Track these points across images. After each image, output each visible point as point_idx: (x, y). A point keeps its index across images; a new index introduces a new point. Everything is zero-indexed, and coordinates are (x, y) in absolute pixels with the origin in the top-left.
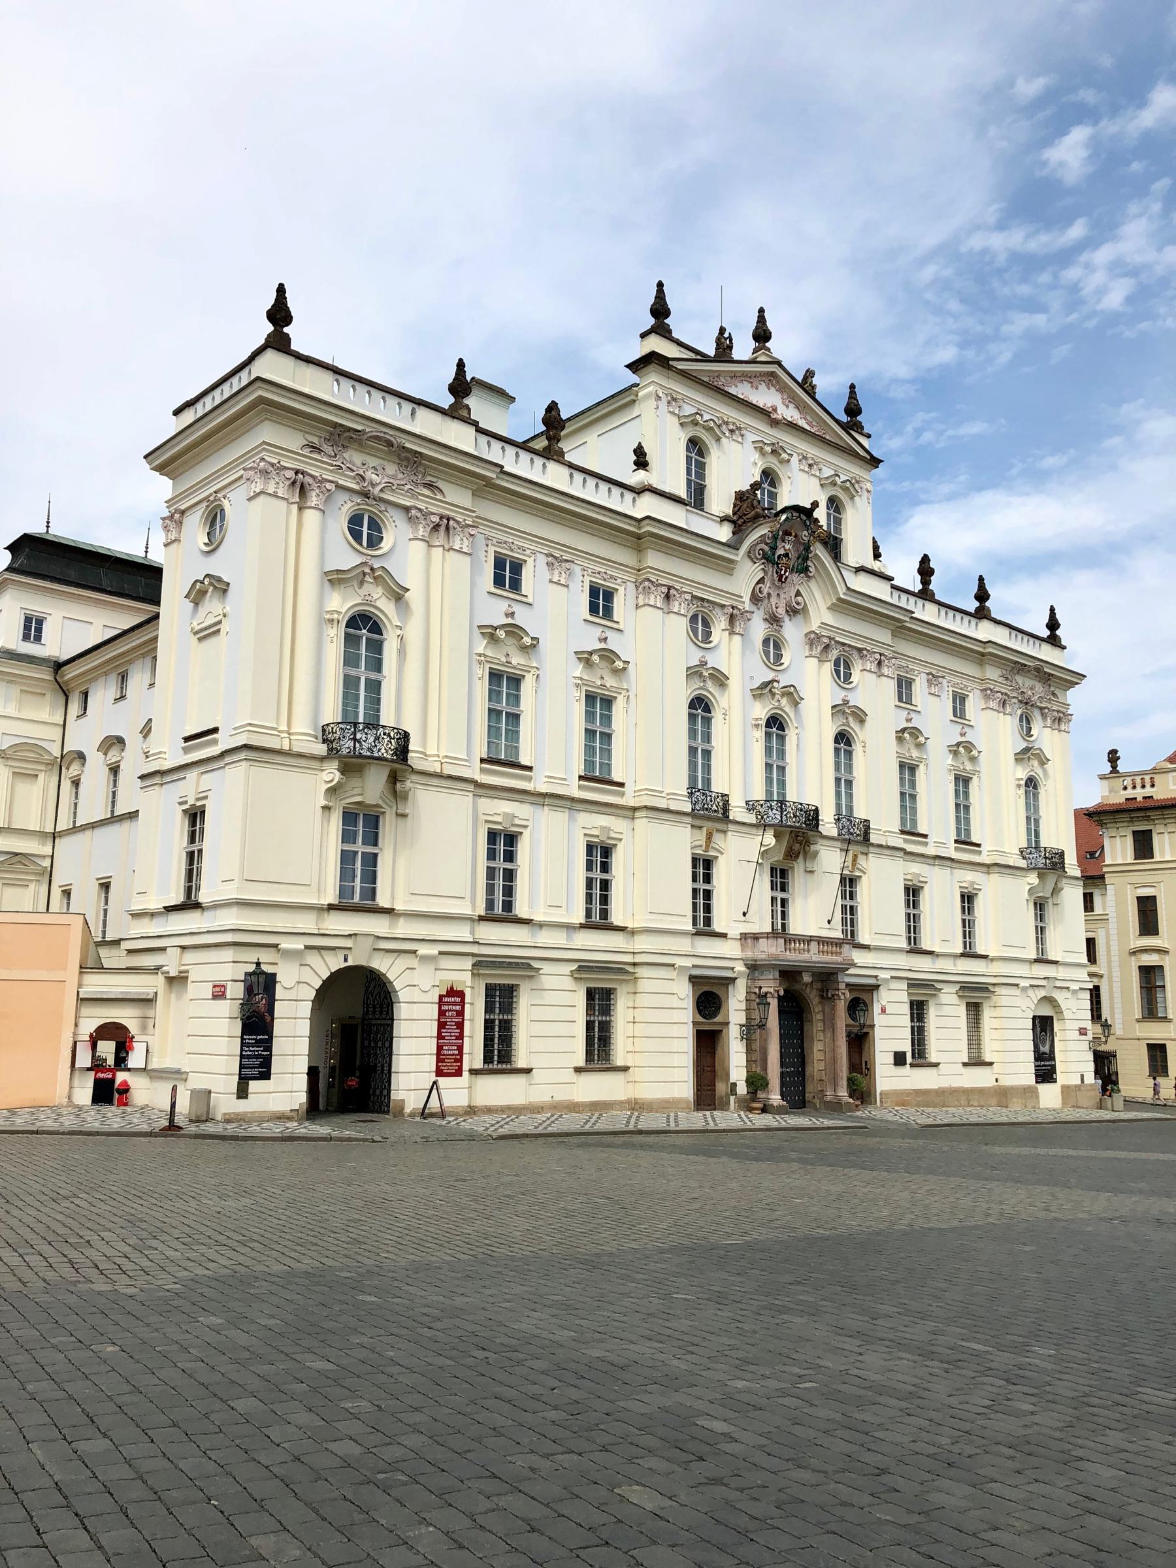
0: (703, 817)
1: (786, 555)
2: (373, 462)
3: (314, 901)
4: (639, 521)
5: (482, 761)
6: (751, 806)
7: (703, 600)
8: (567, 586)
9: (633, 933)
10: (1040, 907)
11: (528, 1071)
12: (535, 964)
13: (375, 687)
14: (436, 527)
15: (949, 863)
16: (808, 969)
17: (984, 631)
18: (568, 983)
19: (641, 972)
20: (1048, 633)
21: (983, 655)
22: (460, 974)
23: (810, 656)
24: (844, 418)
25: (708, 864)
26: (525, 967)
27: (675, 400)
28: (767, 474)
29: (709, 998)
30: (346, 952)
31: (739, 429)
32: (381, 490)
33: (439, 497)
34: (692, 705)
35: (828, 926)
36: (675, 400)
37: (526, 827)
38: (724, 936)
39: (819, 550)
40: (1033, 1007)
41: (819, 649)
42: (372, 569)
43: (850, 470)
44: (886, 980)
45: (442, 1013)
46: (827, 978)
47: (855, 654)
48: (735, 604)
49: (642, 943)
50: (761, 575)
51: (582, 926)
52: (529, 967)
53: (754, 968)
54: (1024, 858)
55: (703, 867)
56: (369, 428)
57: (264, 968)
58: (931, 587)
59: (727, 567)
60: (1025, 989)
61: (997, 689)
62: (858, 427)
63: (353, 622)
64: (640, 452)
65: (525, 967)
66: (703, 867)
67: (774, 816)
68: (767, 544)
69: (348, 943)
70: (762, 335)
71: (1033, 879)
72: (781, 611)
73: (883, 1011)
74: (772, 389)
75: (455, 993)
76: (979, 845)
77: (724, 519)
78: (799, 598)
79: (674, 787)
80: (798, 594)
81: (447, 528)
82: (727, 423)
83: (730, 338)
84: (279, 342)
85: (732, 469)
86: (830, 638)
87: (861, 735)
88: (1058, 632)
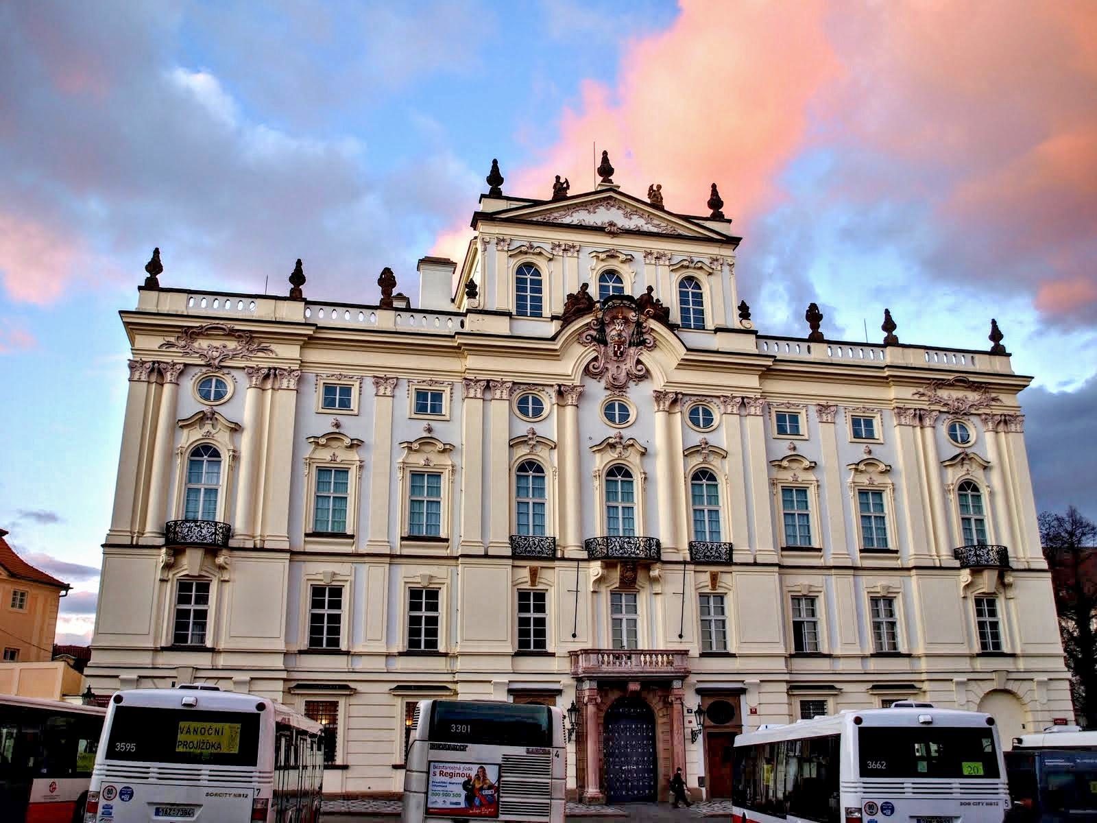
1: (619, 335)
3: (151, 645)
4: (453, 337)
5: (307, 535)
6: (588, 545)
7: (529, 384)
8: (393, 397)
9: (455, 656)
10: (986, 605)
11: (345, 767)
12: (352, 685)
13: (212, 492)
14: (267, 377)
15: (852, 572)
16: (635, 679)
18: (388, 699)
20: (992, 344)
23: (659, 411)
24: (708, 212)
25: (540, 597)
26: (345, 688)
27: (503, 240)
28: (610, 275)
30: (174, 680)
31: (574, 247)
32: (221, 361)
33: (272, 355)
34: (522, 468)
35: (679, 640)
36: (503, 240)
37: (347, 581)
38: (553, 655)
39: (653, 324)
40: (978, 701)
41: (667, 403)
42: (213, 413)
43: (703, 252)
44: (750, 684)
46: (661, 685)
47: (715, 400)
48: (560, 382)
49: (460, 664)
50: (596, 354)
51: (401, 654)
52: (346, 687)
53: (580, 680)
54: (956, 558)
55: (531, 601)
56: (205, 323)
57: (93, 691)
58: (819, 330)
59: (553, 355)
60: (958, 683)
61: (908, 406)
62: (718, 217)
66: (531, 601)
67: (601, 550)
68: (595, 330)
69: (173, 673)
70: (606, 170)
71: (965, 576)
74: (613, 210)
76: (896, 552)
77: (553, 318)
78: (639, 367)
79: (499, 538)
80: (639, 362)
81: (275, 375)
82: (559, 246)
83: (567, 181)
84: (151, 285)
85: (563, 278)
86: (677, 394)
87: (723, 470)
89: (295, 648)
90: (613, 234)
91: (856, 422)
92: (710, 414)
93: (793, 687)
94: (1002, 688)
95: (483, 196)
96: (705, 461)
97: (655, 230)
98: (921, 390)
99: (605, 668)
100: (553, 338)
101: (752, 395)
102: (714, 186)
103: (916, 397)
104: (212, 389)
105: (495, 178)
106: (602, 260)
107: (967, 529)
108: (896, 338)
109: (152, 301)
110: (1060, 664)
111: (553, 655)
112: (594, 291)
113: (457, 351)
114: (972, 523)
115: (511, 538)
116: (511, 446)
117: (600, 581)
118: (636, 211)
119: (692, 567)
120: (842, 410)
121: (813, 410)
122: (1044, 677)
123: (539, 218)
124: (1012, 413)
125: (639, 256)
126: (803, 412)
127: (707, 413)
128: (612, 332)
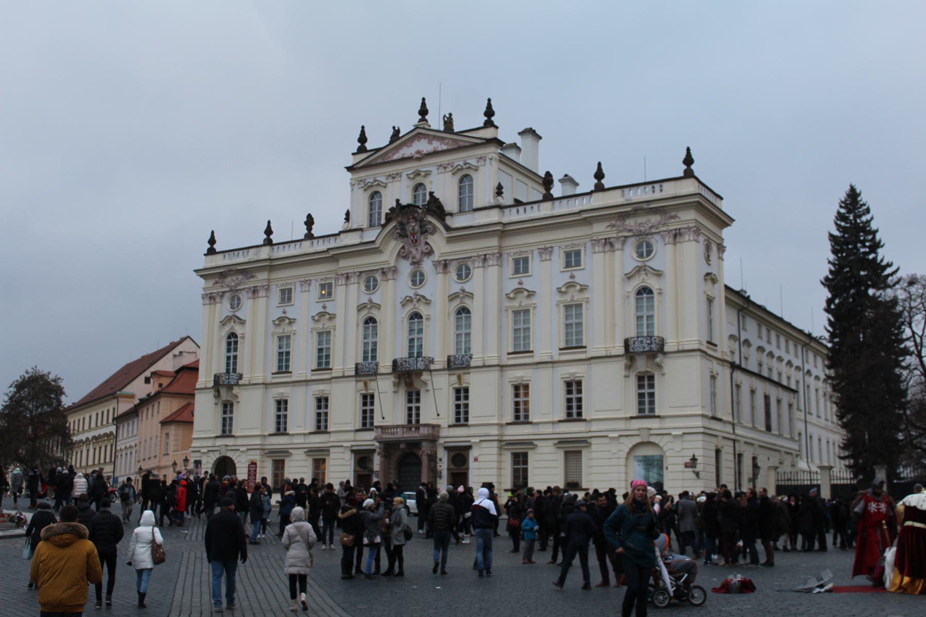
0: (361, 376)
1: (413, 229)
2: (234, 278)
15: (550, 365)
17: (599, 200)
18: (303, 457)
19: (332, 450)
21: (585, 219)
22: (256, 456)
25: (372, 396)
26: (286, 452)
28: (419, 187)
29: (362, 458)
39: (430, 218)
40: (627, 450)
45: (249, 471)
50: (401, 245)
55: (368, 399)
60: (612, 438)
61: (600, 237)
62: (489, 124)
63: (229, 337)
64: (348, 214)
65: (286, 452)
66: (368, 399)
70: (423, 112)
72: (418, 256)
73: (476, 460)
75: (253, 464)
80: (427, 243)
82: (390, 176)
84: (211, 252)
88: (693, 167)
89: (266, 433)
90: (419, 159)
91: (568, 255)
92: (469, 269)
93: (503, 444)
94: (646, 440)
95: (353, 154)
96: (461, 302)
97: (445, 147)
98: (613, 222)
99: (384, 436)
100: (373, 242)
101: (490, 252)
102: (489, 100)
103: (609, 229)
104: (236, 303)
105: (363, 139)
106: (413, 178)
107: (639, 326)
108: (603, 185)
109: (218, 261)
110: (699, 423)
111: (372, 430)
112: (406, 200)
113: (335, 258)
114: (645, 319)
115: (357, 364)
116: (359, 311)
117: (396, 385)
118: (435, 137)
119: (447, 372)
120: (556, 249)
121: (536, 252)
122: (679, 432)
123: (380, 161)
124: (685, 226)
125: (433, 169)
126: (530, 256)
127: (468, 269)
128: (409, 228)
